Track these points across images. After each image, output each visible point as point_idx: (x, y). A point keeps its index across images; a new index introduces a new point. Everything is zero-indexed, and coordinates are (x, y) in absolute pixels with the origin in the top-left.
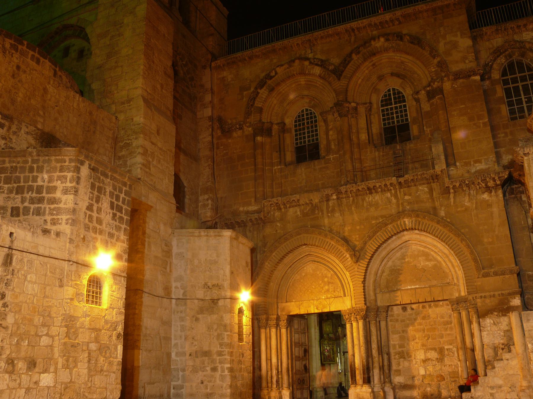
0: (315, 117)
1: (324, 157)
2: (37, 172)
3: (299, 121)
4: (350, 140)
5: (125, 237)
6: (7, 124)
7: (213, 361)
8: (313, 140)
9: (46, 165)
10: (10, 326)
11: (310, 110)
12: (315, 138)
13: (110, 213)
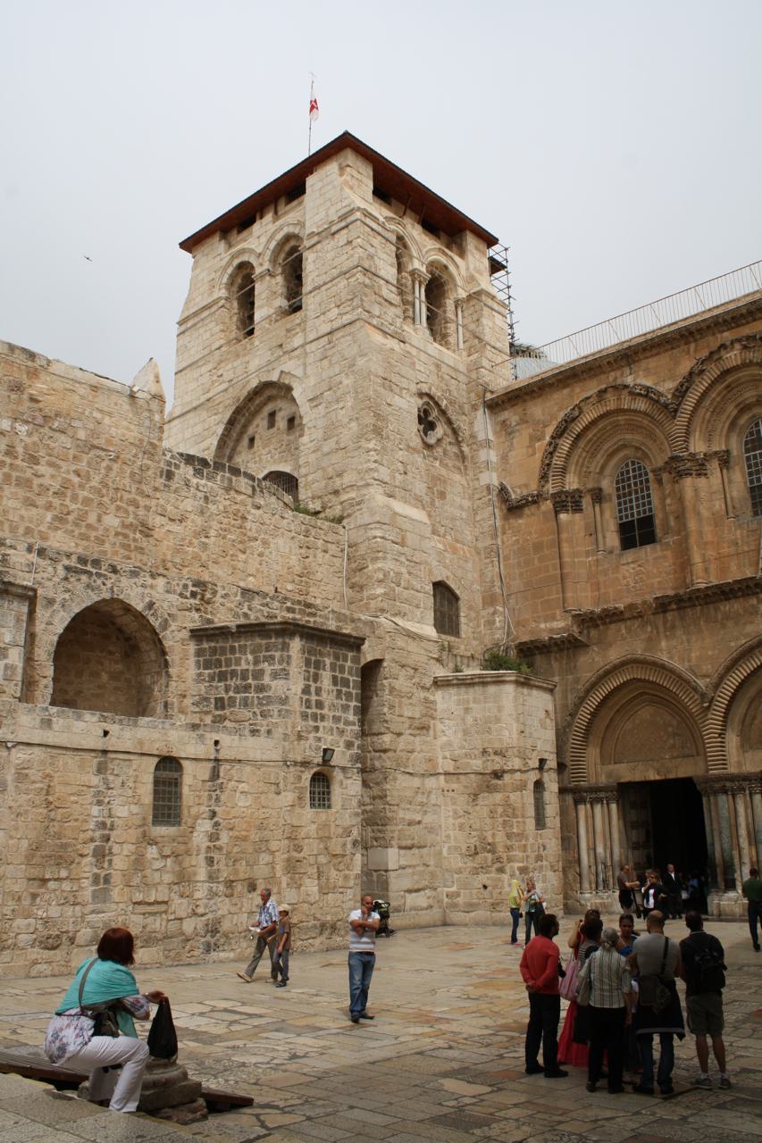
0: (646, 474)
1: (661, 541)
2: (240, 652)
3: (623, 481)
4: (698, 514)
6: (198, 590)
7: (498, 859)
8: (644, 512)
9: (249, 643)
11: (638, 463)
12: (647, 507)
13: (332, 691)
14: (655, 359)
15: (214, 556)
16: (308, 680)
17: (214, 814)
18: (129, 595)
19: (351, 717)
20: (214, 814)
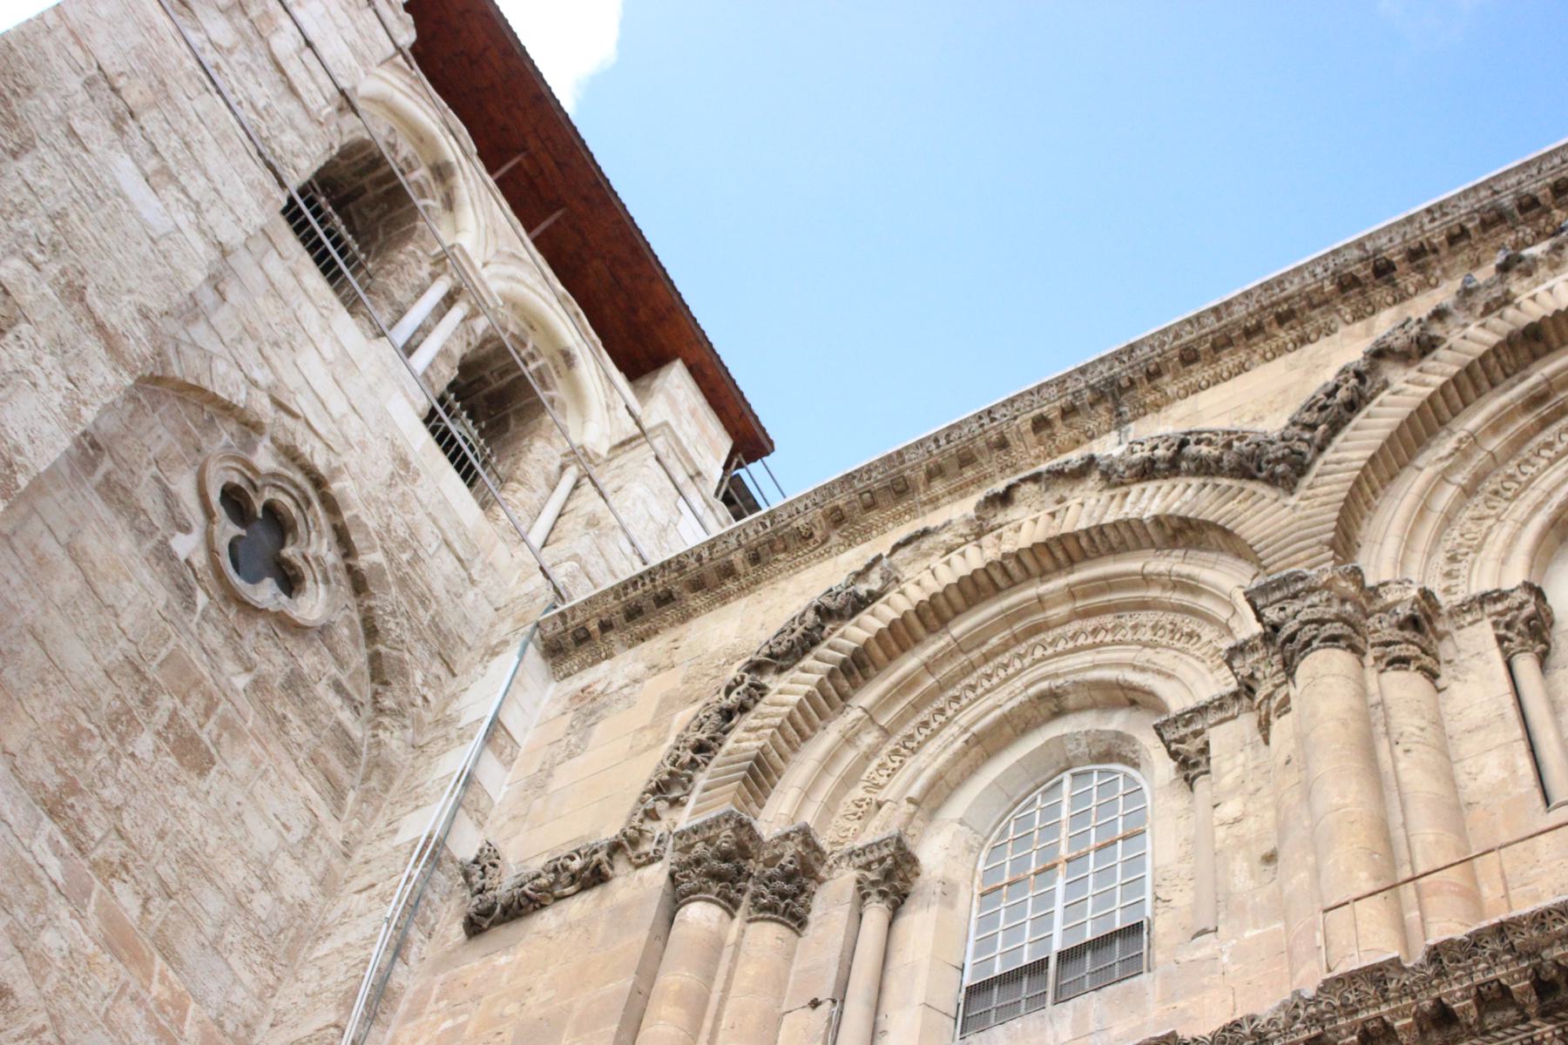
14: (1224, 387)
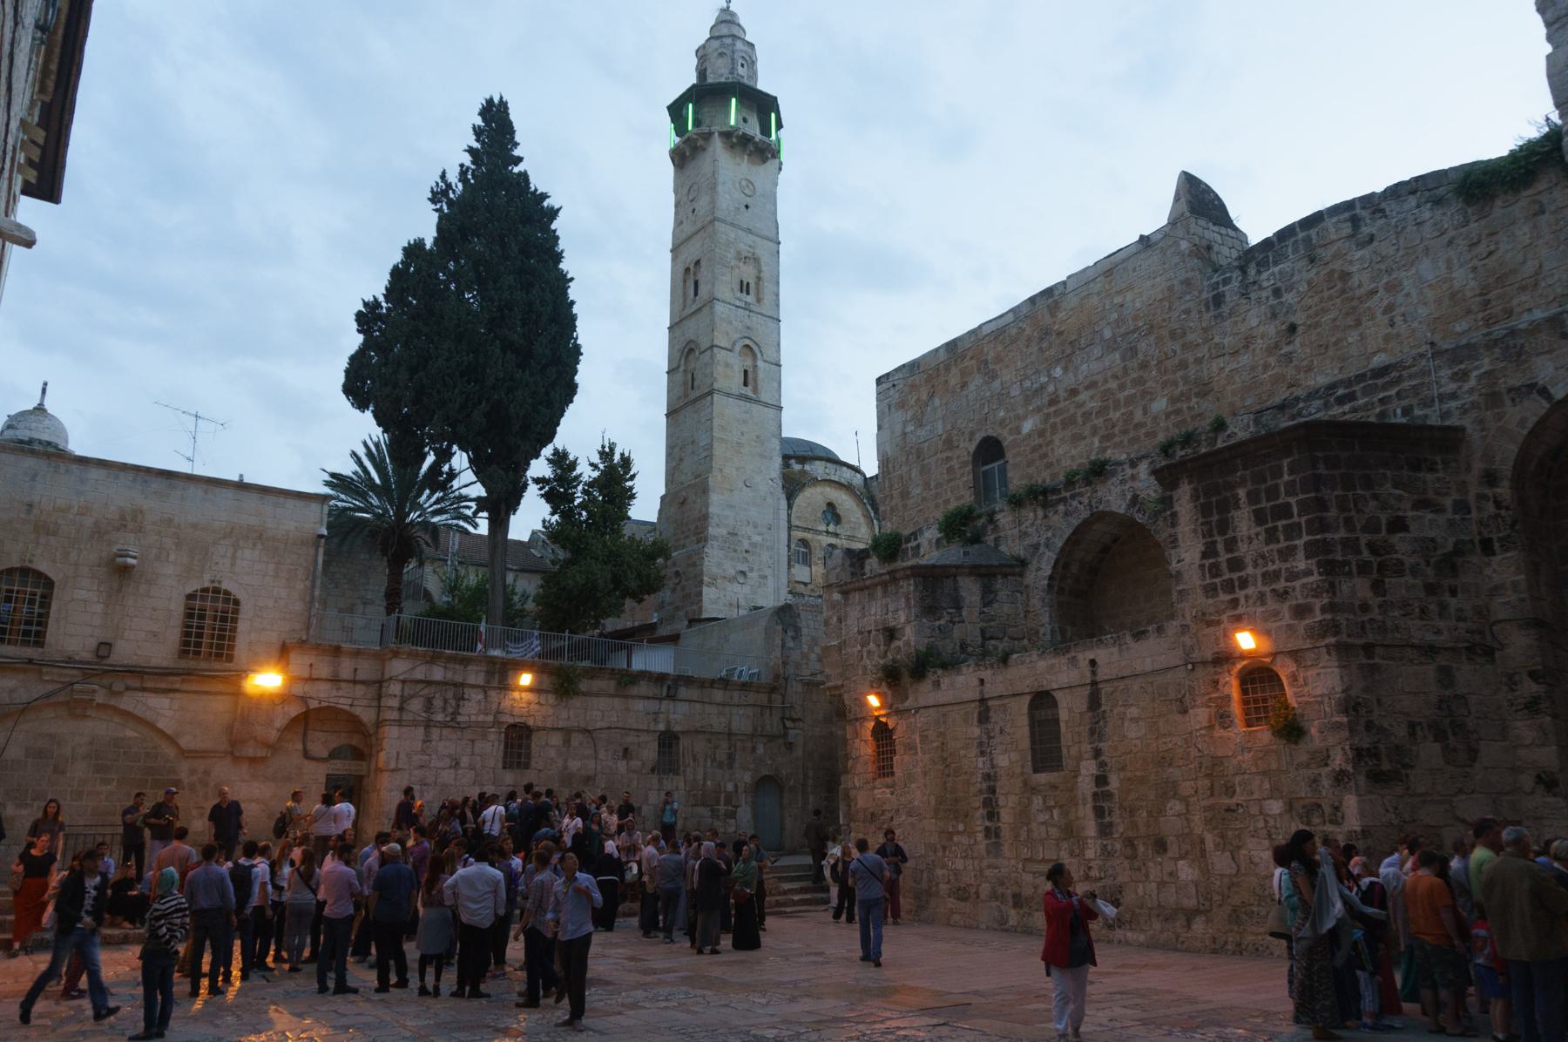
5: (1309, 562)
10: (1116, 791)
15: (1305, 363)
16: (1211, 535)
17: (1097, 753)
18: (1108, 501)
19: (1301, 563)
20: (1097, 753)
